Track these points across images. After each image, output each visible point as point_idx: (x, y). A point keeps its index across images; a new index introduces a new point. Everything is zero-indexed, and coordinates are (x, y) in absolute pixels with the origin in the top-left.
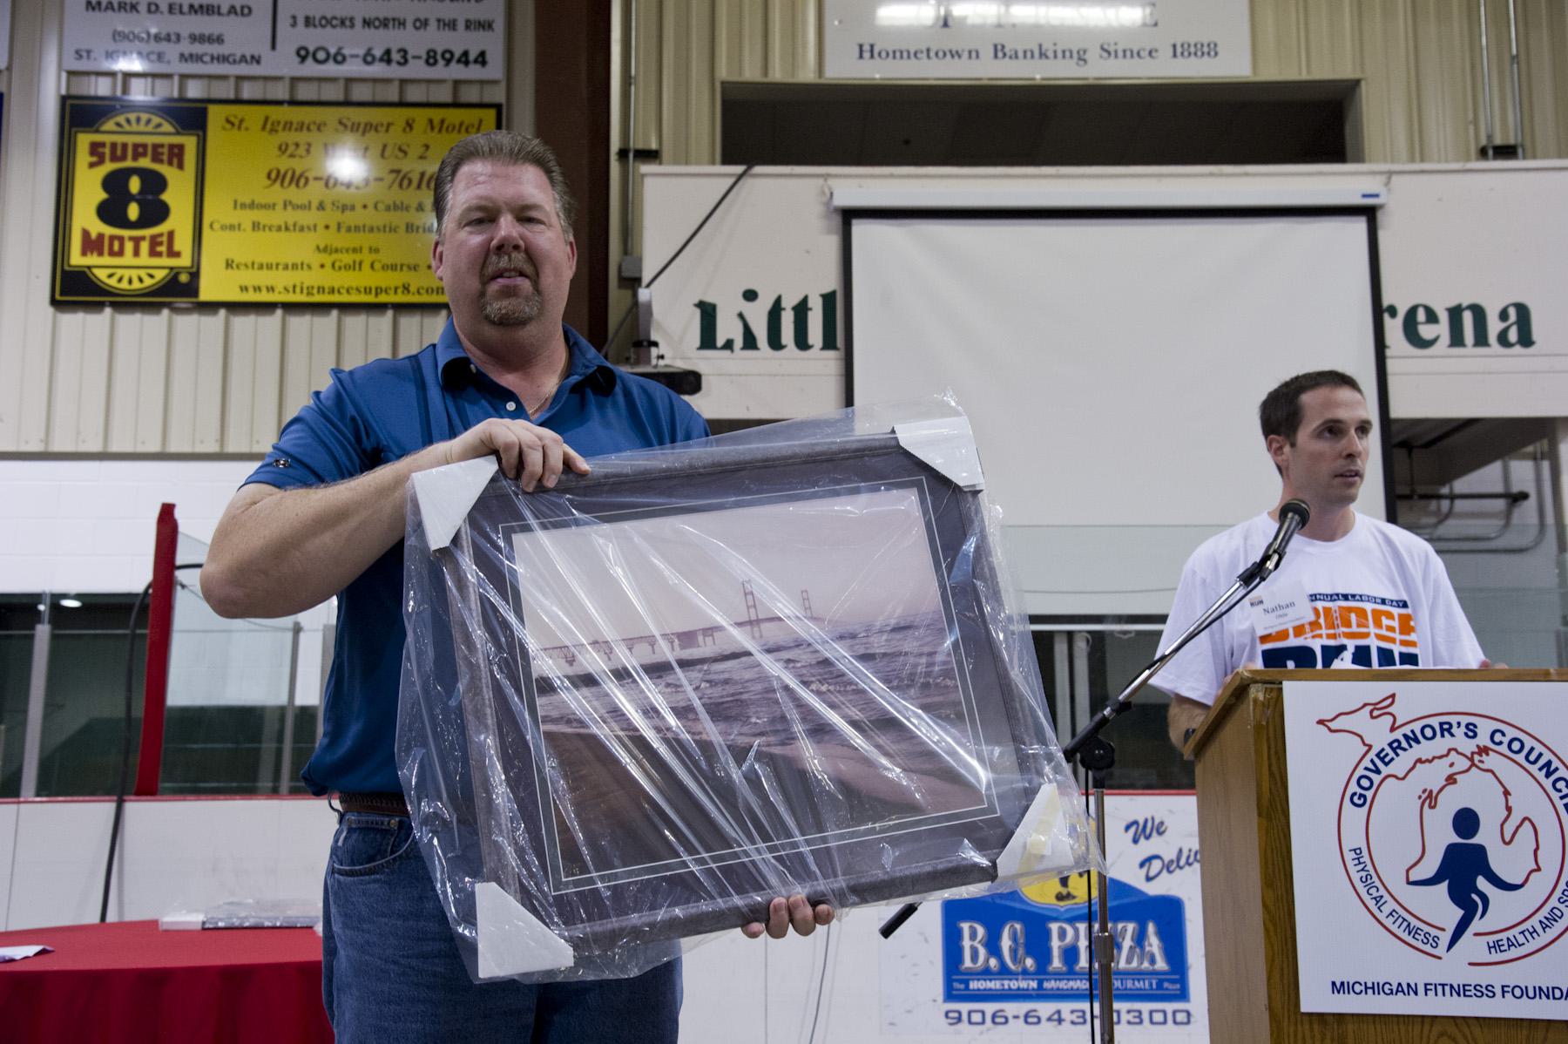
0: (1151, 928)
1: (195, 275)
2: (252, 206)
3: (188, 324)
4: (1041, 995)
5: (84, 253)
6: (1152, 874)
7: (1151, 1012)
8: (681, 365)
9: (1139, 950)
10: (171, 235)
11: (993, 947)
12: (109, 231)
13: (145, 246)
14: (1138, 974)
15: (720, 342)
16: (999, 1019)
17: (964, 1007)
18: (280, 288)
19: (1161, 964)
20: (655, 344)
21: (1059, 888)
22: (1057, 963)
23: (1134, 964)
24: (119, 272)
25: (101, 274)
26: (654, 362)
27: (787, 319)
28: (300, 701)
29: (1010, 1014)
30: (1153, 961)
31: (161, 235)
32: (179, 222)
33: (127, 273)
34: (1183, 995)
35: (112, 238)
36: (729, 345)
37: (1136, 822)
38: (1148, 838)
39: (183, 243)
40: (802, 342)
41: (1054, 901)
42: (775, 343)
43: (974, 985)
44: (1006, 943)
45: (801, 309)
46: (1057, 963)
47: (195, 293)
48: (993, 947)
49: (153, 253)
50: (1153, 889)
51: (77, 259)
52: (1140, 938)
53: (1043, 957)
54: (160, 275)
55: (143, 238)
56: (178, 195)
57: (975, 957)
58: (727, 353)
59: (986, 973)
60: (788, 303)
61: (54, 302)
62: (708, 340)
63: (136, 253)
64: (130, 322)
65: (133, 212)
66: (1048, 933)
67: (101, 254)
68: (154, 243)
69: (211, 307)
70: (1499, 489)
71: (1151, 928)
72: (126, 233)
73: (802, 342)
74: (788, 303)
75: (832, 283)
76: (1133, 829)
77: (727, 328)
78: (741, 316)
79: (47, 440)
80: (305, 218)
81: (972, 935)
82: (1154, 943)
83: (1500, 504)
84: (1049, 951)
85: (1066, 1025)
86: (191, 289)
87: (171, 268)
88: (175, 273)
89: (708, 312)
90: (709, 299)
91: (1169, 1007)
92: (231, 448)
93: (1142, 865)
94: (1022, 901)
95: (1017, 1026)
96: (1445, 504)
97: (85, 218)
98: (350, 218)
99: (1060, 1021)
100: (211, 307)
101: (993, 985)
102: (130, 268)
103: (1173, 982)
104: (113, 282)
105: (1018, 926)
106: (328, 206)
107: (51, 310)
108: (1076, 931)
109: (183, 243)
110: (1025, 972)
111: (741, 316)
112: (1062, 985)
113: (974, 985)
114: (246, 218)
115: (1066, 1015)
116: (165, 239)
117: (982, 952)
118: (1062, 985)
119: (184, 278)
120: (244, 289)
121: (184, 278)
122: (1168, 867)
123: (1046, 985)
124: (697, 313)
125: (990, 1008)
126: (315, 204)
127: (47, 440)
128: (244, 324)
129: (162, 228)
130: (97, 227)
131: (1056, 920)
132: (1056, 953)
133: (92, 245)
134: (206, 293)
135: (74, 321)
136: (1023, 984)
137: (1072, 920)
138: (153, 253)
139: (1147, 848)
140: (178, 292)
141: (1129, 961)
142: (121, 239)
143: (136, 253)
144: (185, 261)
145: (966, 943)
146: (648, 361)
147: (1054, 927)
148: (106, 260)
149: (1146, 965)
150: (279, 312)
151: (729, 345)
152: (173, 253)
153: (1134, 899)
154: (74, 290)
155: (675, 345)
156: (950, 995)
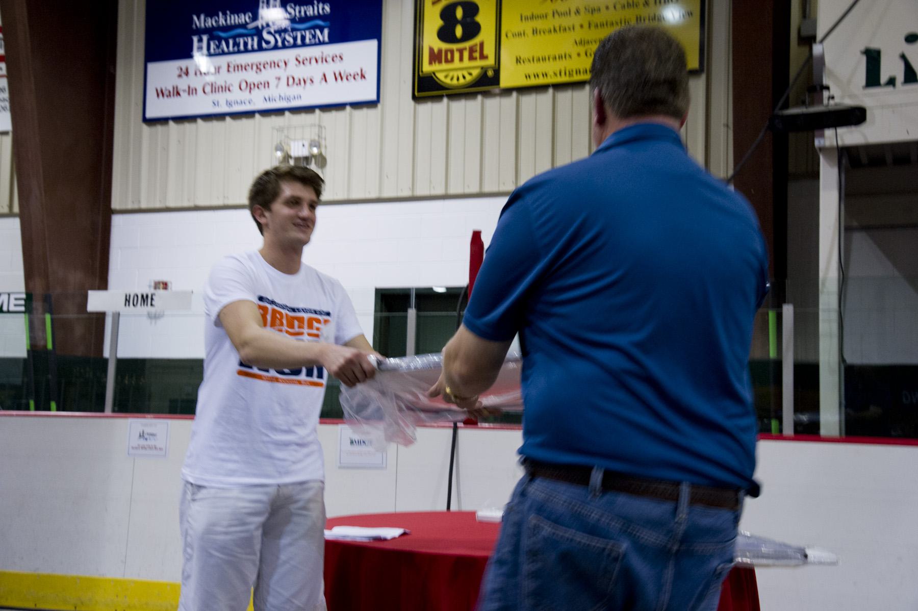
1: (497, 72)
2: (533, 17)
3: (492, 104)
5: (430, 63)
8: (849, 102)
10: (482, 45)
12: (444, 46)
13: (466, 54)
15: (884, 78)
18: (551, 73)
20: (828, 88)
24: (451, 74)
25: (441, 76)
26: (825, 101)
31: (476, 45)
32: (487, 35)
33: (455, 74)
35: (446, 51)
36: (892, 82)
39: (489, 50)
49: (471, 58)
51: (427, 68)
54: (476, 73)
55: (465, 49)
56: (485, 19)
58: (890, 89)
61: (414, 98)
62: (873, 79)
63: (461, 59)
64: (459, 107)
65: (459, 31)
67: (440, 62)
68: (472, 51)
69: (508, 91)
72: (454, 47)
77: (891, 67)
78: (903, 57)
80: (566, 22)
86: (496, 80)
87: (482, 68)
88: (484, 70)
90: (874, 45)
97: (431, 40)
98: (597, 18)
100: (508, 91)
102: (457, 71)
104: (448, 81)
106: (582, 10)
107: (412, 103)
109: (489, 50)
111: (903, 57)
114: (528, 26)
116: (478, 49)
119: (490, 73)
120: (528, 77)
121: (490, 73)
126: (573, 10)
128: (528, 100)
129: (476, 41)
130: (438, 45)
133: (435, 57)
135: (427, 108)
140: (486, 84)
142: (452, 52)
143: (461, 59)
146: (821, 101)
148: (444, 66)
150: (551, 91)
151: (892, 82)
152: (483, 57)
154: (426, 88)
155: (843, 84)
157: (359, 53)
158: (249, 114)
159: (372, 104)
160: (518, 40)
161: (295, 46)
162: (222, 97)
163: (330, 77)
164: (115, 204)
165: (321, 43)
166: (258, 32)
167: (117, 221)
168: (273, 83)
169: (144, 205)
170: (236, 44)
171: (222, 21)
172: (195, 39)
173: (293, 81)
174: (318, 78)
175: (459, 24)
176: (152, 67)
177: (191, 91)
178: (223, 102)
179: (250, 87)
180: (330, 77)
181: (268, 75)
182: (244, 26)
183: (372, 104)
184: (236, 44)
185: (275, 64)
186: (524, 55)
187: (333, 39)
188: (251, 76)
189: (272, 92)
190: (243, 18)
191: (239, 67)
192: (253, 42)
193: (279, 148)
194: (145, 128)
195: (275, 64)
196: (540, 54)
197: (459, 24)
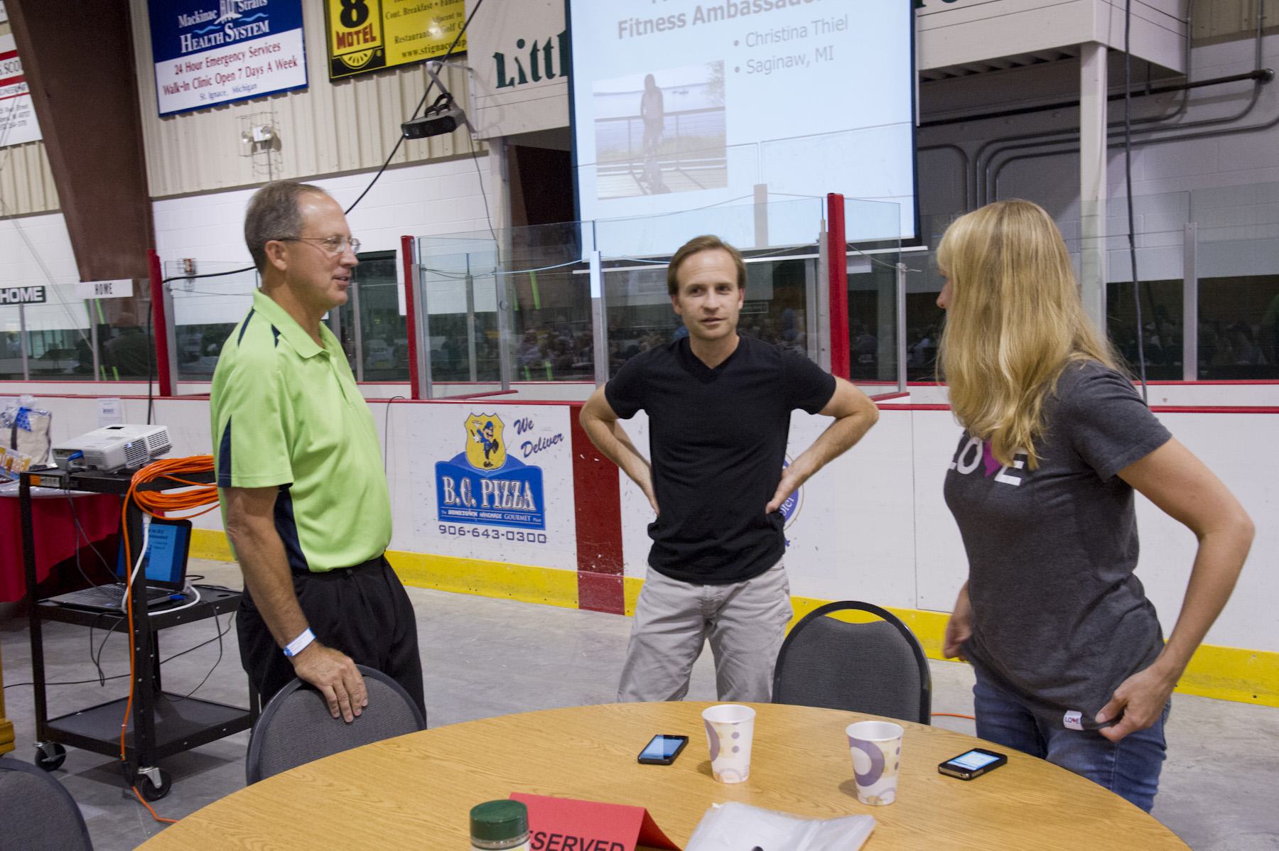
0: (527, 485)
1: (383, 51)
4: (480, 521)
9: (514, 497)
11: (457, 490)
12: (347, 30)
13: (361, 35)
14: (521, 512)
15: (508, 81)
16: (462, 532)
17: (447, 524)
19: (532, 507)
21: (484, 459)
22: (485, 503)
25: (346, 58)
27: (541, 56)
28: (479, 308)
32: (373, 18)
36: (512, 83)
39: (376, 33)
40: (550, 75)
42: (536, 77)
43: (450, 512)
44: (463, 490)
45: (548, 48)
46: (485, 503)
47: (384, 63)
48: (457, 490)
50: (528, 462)
51: (337, 52)
52: (522, 490)
53: (479, 498)
54: (369, 53)
58: (510, 88)
59: (455, 506)
60: (541, 46)
61: (331, 81)
66: (480, 485)
68: (365, 34)
70: (1250, 68)
71: (527, 485)
72: (353, 30)
73: (550, 75)
74: (541, 46)
75: (562, 29)
77: (511, 72)
78: (516, 59)
79: (339, 165)
81: (449, 482)
82: (529, 495)
83: (1250, 83)
89: (499, 58)
90: (501, 51)
91: (537, 532)
92: (436, 155)
96: (1180, 95)
97: (338, 27)
101: (458, 513)
102: (356, 55)
104: (351, 63)
109: (376, 33)
111: (516, 59)
112: (488, 515)
113: (450, 512)
118: (488, 515)
119: (379, 53)
120: (404, 55)
124: (494, 62)
125: (458, 525)
127: (339, 165)
129: (366, 24)
132: (485, 497)
133: (342, 41)
134: (389, 63)
137: (491, 479)
138: (366, 41)
139: (526, 436)
140: (377, 65)
142: (350, 34)
144: (377, 43)
145: (446, 488)
147: (483, 481)
152: (373, 39)
154: (339, 72)
156: (441, 518)
157: (290, 40)
158: (224, 105)
159: (302, 88)
160: (394, 19)
161: (247, 39)
162: (206, 90)
163: (274, 66)
164: (152, 193)
165: (265, 35)
166: (222, 26)
167: (157, 206)
168: (237, 73)
169: (170, 193)
170: (210, 40)
171: (198, 21)
172: (183, 37)
173: (253, 72)
174: (265, 68)
175: (354, 7)
176: (159, 65)
177: (186, 86)
178: (207, 96)
179: (224, 79)
180: (274, 66)
181: (233, 67)
182: (211, 22)
183: (302, 88)
184: (210, 40)
185: (236, 57)
186: (401, 36)
187: (274, 30)
188: (223, 70)
189: (215, 88)
190: (211, 15)
191: (214, 62)
192: (220, 37)
193: (244, 136)
194: (162, 122)
195: (236, 57)
196: (411, 34)
197: (354, 7)
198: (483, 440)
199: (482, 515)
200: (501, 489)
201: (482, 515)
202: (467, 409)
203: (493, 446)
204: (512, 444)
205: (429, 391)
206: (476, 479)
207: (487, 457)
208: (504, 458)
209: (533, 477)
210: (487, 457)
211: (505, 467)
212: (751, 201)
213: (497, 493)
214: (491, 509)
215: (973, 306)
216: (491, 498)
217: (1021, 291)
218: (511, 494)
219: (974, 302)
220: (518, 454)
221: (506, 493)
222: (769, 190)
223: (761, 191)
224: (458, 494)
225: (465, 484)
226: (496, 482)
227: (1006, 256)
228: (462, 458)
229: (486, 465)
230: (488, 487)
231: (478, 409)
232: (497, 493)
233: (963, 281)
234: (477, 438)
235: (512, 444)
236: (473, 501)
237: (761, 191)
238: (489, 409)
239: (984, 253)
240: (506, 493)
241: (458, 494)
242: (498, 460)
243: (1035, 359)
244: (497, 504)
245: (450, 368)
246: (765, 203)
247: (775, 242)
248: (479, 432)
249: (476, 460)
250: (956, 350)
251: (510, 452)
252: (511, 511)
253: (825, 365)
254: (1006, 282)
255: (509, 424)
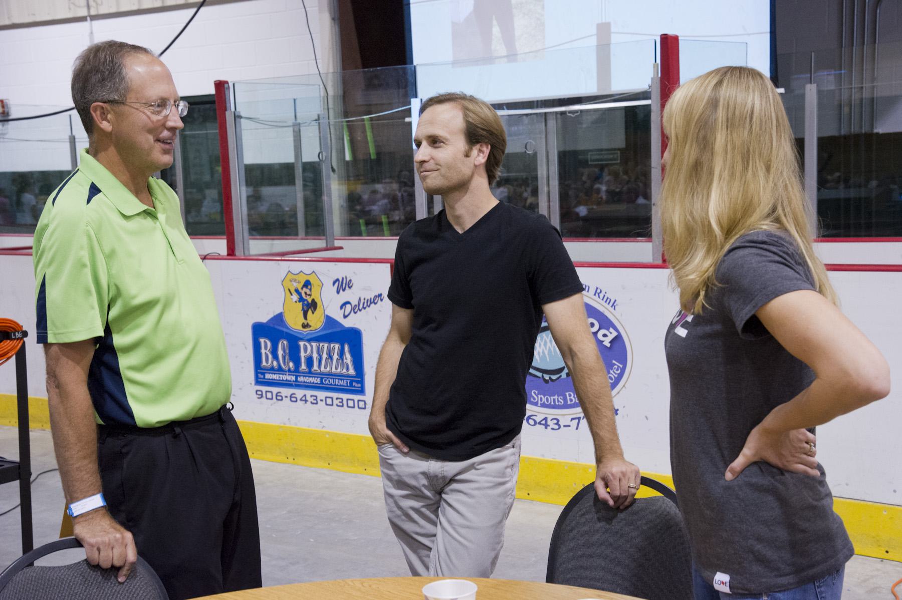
0: (347, 348)
4: (298, 385)
6: (346, 314)
7: (348, 400)
9: (332, 360)
11: (274, 352)
17: (264, 389)
19: (352, 371)
21: (304, 321)
22: (303, 366)
23: (339, 370)
29: (283, 395)
30: (348, 369)
34: (362, 391)
37: (338, 280)
38: (344, 290)
41: (301, 328)
43: (268, 376)
44: (280, 353)
46: (303, 366)
48: (274, 352)
50: (347, 323)
52: (341, 354)
53: (296, 360)
57: (267, 361)
59: (272, 370)
66: (298, 347)
71: (347, 348)
76: (336, 284)
82: (348, 358)
84: (299, 358)
85: (309, 403)
91: (356, 397)
93: (341, 308)
94: (288, 328)
95: (287, 401)
99: (306, 401)
101: (275, 377)
103: (357, 382)
105: (285, 343)
108: (312, 347)
110: (289, 370)
112: (306, 379)
113: (268, 376)
115: (308, 398)
117: (270, 356)
118: (306, 379)
122: (355, 310)
123: (293, 378)
125: (275, 390)
131: (302, 339)
132: (303, 360)
136: (289, 378)
137: (309, 341)
139: (345, 296)
141: (336, 368)
145: (263, 351)
147: (302, 344)
149: (344, 370)
153: (338, 329)
156: (258, 382)
198: (301, 299)
199: (300, 379)
200: (319, 352)
201: (300, 379)
202: (284, 267)
203: (310, 306)
204: (331, 304)
205: (245, 248)
206: (294, 341)
207: (305, 318)
208: (322, 319)
209: (352, 339)
210: (305, 318)
211: (324, 328)
212: (593, 41)
213: (315, 355)
214: (310, 373)
215: (685, 162)
216: (309, 361)
217: (734, 149)
218: (330, 357)
219: (686, 158)
220: (337, 315)
221: (325, 356)
222: (613, 30)
223: (604, 30)
224: (275, 357)
225: (282, 344)
226: (314, 344)
227: (721, 114)
228: (279, 318)
229: (305, 326)
230: (307, 349)
231: (296, 267)
232: (315, 355)
233: (680, 139)
234: (295, 297)
235: (331, 304)
236: (291, 365)
237: (604, 30)
238: (307, 267)
239: (700, 111)
240: (325, 356)
241: (275, 357)
242: (316, 321)
243: (739, 215)
244: (315, 367)
245: (272, 225)
246: (609, 45)
247: (619, 86)
248: (297, 291)
249: (294, 321)
250: (668, 206)
251: (328, 313)
252: (330, 375)
253: (556, 222)
254: (720, 139)
255: (328, 282)
